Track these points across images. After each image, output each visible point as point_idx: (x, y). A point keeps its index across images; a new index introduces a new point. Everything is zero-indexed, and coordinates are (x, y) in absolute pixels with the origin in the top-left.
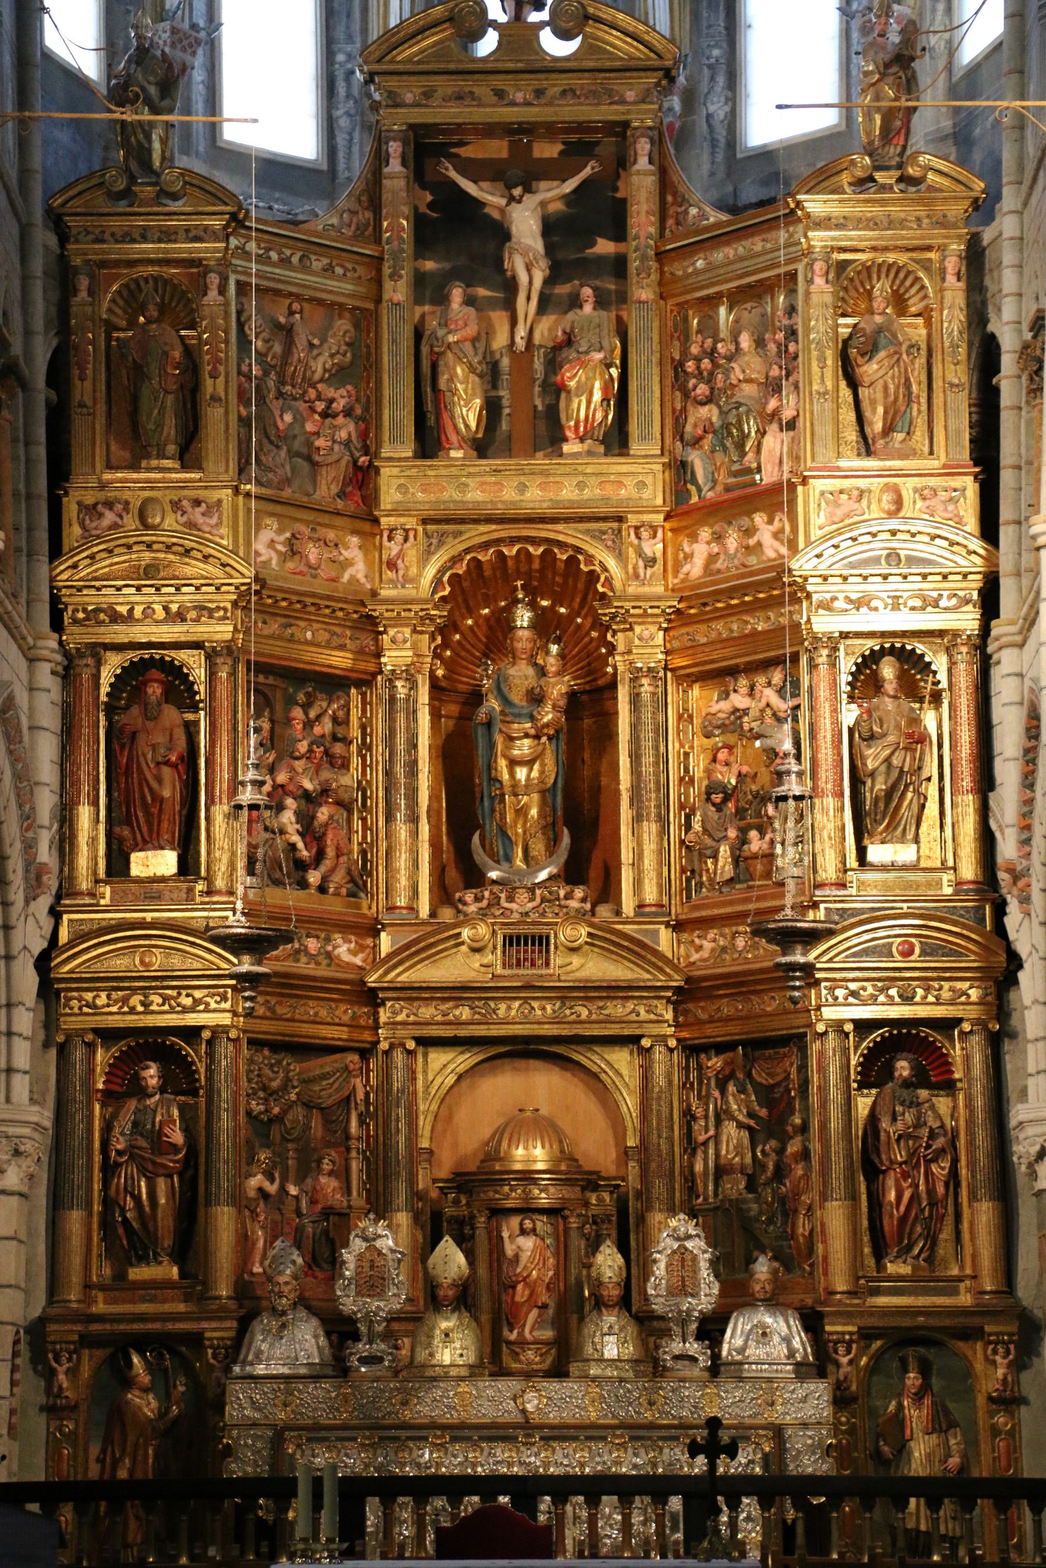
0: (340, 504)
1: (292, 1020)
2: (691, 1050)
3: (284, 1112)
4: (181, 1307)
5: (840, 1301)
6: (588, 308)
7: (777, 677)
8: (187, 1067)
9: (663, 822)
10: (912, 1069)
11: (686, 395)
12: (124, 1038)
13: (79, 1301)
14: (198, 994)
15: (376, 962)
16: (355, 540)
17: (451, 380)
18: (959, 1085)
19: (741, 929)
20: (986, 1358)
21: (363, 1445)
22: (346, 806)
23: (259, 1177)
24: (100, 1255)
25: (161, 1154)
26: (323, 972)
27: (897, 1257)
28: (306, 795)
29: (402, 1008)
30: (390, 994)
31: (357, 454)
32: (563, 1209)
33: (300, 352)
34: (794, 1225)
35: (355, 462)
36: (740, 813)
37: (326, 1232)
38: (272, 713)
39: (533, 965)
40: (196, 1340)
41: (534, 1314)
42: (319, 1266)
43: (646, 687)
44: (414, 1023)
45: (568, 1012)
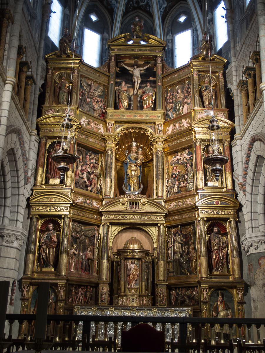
0: (99, 117)
1: (83, 216)
2: (169, 228)
3: (81, 236)
4: (54, 277)
5: (204, 279)
6: (148, 87)
7: (187, 151)
8: (58, 224)
9: (163, 179)
10: (218, 230)
11: (167, 103)
12: (45, 218)
13: (30, 275)
14: (62, 208)
15: (102, 205)
16: (101, 125)
17: (122, 97)
18: (228, 233)
19: (180, 201)
20: (237, 293)
21: (93, 310)
22: (97, 176)
23: (74, 250)
24: (37, 266)
25: (52, 243)
26: (90, 207)
27: (216, 270)
28: (89, 173)
29: (107, 216)
30: (104, 213)
31: (103, 109)
32: (141, 258)
33: (93, 90)
34: (191, 264)
35: (102, 111)
36: (178, 180)
37: (88, 263)
38: (82, 156)
39: (135, 208)
40: (56, 285)
41: (134, 282)
42: (86, 271)
43: (160, 154)
44: (110, 219)
45: (142, 218)
